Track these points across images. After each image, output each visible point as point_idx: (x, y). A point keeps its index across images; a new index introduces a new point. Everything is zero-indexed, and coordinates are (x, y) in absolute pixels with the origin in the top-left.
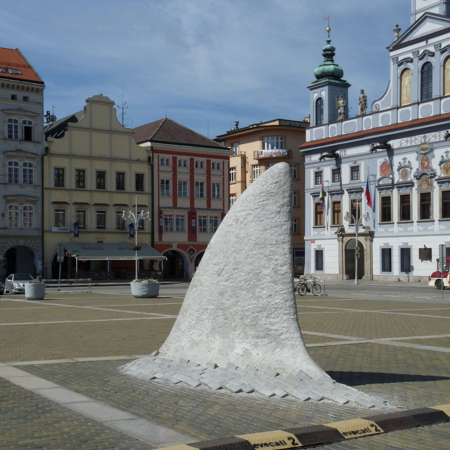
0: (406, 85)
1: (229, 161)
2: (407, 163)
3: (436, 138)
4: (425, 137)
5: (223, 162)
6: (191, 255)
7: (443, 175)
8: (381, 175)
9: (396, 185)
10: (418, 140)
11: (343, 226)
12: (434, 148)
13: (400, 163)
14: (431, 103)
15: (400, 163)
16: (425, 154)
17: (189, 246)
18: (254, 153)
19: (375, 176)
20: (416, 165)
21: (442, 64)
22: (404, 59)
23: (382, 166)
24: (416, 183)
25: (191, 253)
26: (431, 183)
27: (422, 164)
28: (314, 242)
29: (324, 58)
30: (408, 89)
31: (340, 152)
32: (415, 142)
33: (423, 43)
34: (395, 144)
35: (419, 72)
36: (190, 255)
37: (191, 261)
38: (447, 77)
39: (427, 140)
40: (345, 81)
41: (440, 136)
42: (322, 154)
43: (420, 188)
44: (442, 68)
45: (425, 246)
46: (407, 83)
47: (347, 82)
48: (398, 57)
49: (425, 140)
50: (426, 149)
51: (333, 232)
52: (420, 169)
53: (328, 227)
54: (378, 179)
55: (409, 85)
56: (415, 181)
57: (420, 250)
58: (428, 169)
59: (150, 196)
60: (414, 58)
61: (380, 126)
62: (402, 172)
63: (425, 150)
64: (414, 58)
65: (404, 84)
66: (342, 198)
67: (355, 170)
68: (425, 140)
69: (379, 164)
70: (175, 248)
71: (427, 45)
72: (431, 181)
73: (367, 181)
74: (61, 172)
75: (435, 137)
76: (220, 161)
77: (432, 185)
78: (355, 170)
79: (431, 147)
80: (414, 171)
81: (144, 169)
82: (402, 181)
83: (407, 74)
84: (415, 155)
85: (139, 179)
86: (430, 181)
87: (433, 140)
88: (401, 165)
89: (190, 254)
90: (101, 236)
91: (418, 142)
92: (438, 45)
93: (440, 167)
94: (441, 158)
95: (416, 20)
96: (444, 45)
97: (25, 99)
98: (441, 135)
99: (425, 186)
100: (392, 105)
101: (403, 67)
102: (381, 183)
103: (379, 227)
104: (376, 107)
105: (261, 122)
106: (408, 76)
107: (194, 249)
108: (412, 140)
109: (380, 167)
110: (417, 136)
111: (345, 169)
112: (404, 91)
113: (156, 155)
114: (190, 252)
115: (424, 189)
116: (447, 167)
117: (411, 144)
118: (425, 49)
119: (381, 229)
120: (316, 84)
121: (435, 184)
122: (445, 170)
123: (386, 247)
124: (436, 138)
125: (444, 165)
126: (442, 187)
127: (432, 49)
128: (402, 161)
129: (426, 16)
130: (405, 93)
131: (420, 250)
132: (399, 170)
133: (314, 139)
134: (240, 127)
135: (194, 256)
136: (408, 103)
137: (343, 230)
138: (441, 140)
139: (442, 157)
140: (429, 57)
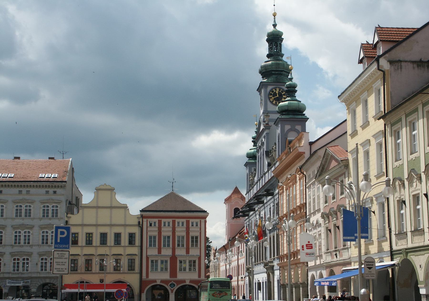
1: (205, 220)
5: (200, 221)
17: (171, 281)
25: (172, 286)
29: (253, 143)
37: (172, 292)
70: (158, 283)
74: (76, 235)
76: (198, 220)
85: (132, 236)
89: (171, 287)
90: (103, 275)
97: (55, 192)
107: (175, 283)
113: (145, 220)
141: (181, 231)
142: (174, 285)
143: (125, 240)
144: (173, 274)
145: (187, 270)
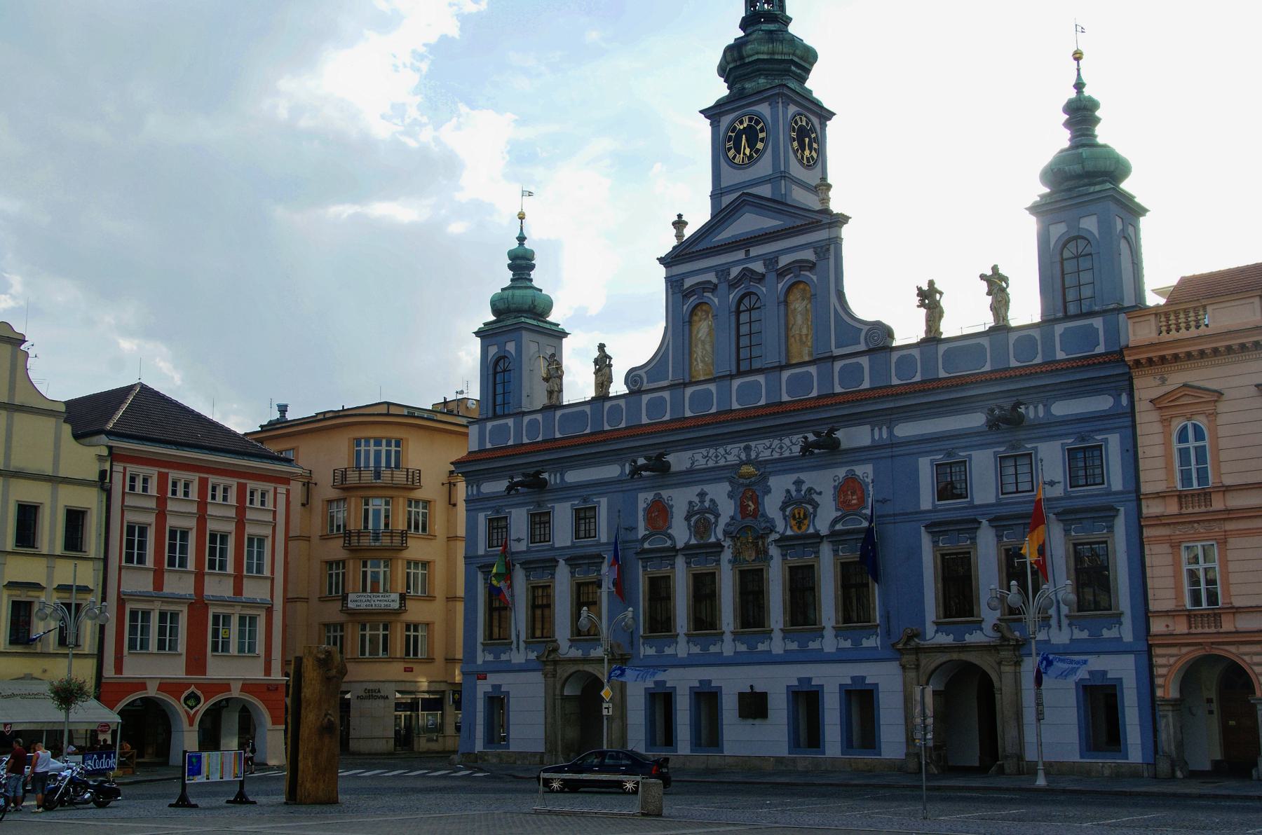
0: (703, 338)
2: (707, 504)
3: (772, 451)
4: (748, 449)
5: (275, 489)
6: (192, 708)
7: (789, 533)
8: (646, 530)
9: (680, 550)
10: (733, 454)
11: (555, 641)
12: (770, 473)
13: (690, 503)
14: (761, 379)
15: (690, 503)
16: (748, 485)
17: (188, 686)
18: (334, 473)
19: (633, 529)
20: (727, 509)
21: (782, 299)
22: (698, 284)
23: (648, 511)
24: (729, 548)
25: (191, 703)
26: (764, 547)
27: (743, 508)
28: (485, 679)
30: (708, 347)
31: (550, 476)
32: (725, 458)
33: (741, 255)
34: (678, 461)
35: (732, 312)
36: (189, 710)
37: (191, 724)
38: (793, 325)
39: (753, 455)
40: (558, 325)
41: (781, 448)
42: (512, 479)
43: (740, 559)
44: (782, 307)
45: (752, 687)
46: (705, 335)
47: (559, 327)
48: (683, 279)
49: (748, 455)
50: (750, 476)
51: (533, 656)
52: (739, 517)
53: (518, 645)
54: (640, 537)
55: (708, 339)
56: (727, 543)
57: (742, 696)
58: (756, 518)
59: (101, 564)
60: (720, 283)
61: (643, 422)
62: (696, 522)
63: (749, 478)
64: (720, 283)
65: (696, 335)
66: (554, 578)
67: (584, 517)
68: (748, 455)
69: (642, 505)
70: (152, 692)
71: (748, 259)
72: (763, 543)
73: (614, 541)
75: (770, 450)
76: (269, 487)
77: (766, 552)
78: (584, 517)
79: (762, 470)
80: (723, 520)
81: (89, 500)
82: (696, 542)
83: (704, 317)
84: (726, 487)
85: (75, 519)
86: (760, 543)
87: (765, 455)
88: (694, 507)
89: (188, 706)
91: (732, 460)
92: (772, 259)
93: (783, 515)
94: (785, 494)
95: (723, 206)
96: (784, 261)
98: (784, 445)
99: (750, 555)
100: (670, 378)
101: (693, 300)
102: (646, 546)
103: (643, 644)
104: (636, 382)
105: (343, 406)
106: (705, 319)
107: (199, 693)
108: (719, 454)
109: (645, 510)
110: (729, 448)
111: (563, 516)
112: (699, 352)
113: (119, 467)
114: (188, 702)
115: (747, 561)
116: (799, 513)
117: (717, 462)
118: (744, 266)
119: (648, 648)
120: (495, 326)
121: (774, 551)
122: (795, 522)
123: (660, 690)
124: (772, 451)
125: (793, 510)
126: (789, 558)
127: (758, 267)
128: (697, 500)
129: (744, 200)
130: (700, 354)
131: (742, 696)
132: (688, 518)
133: (489, 446)
134: (290, 416)
135: (198, 710)
136: (707, 375)
137: (555, 650)
138: (783, 456)
139: (788, 491)
140: (751, 283)
141: (221, 519)
142: (198, 700)
143: (51, 532)
144: (196, 662)
145: (234, 649)
